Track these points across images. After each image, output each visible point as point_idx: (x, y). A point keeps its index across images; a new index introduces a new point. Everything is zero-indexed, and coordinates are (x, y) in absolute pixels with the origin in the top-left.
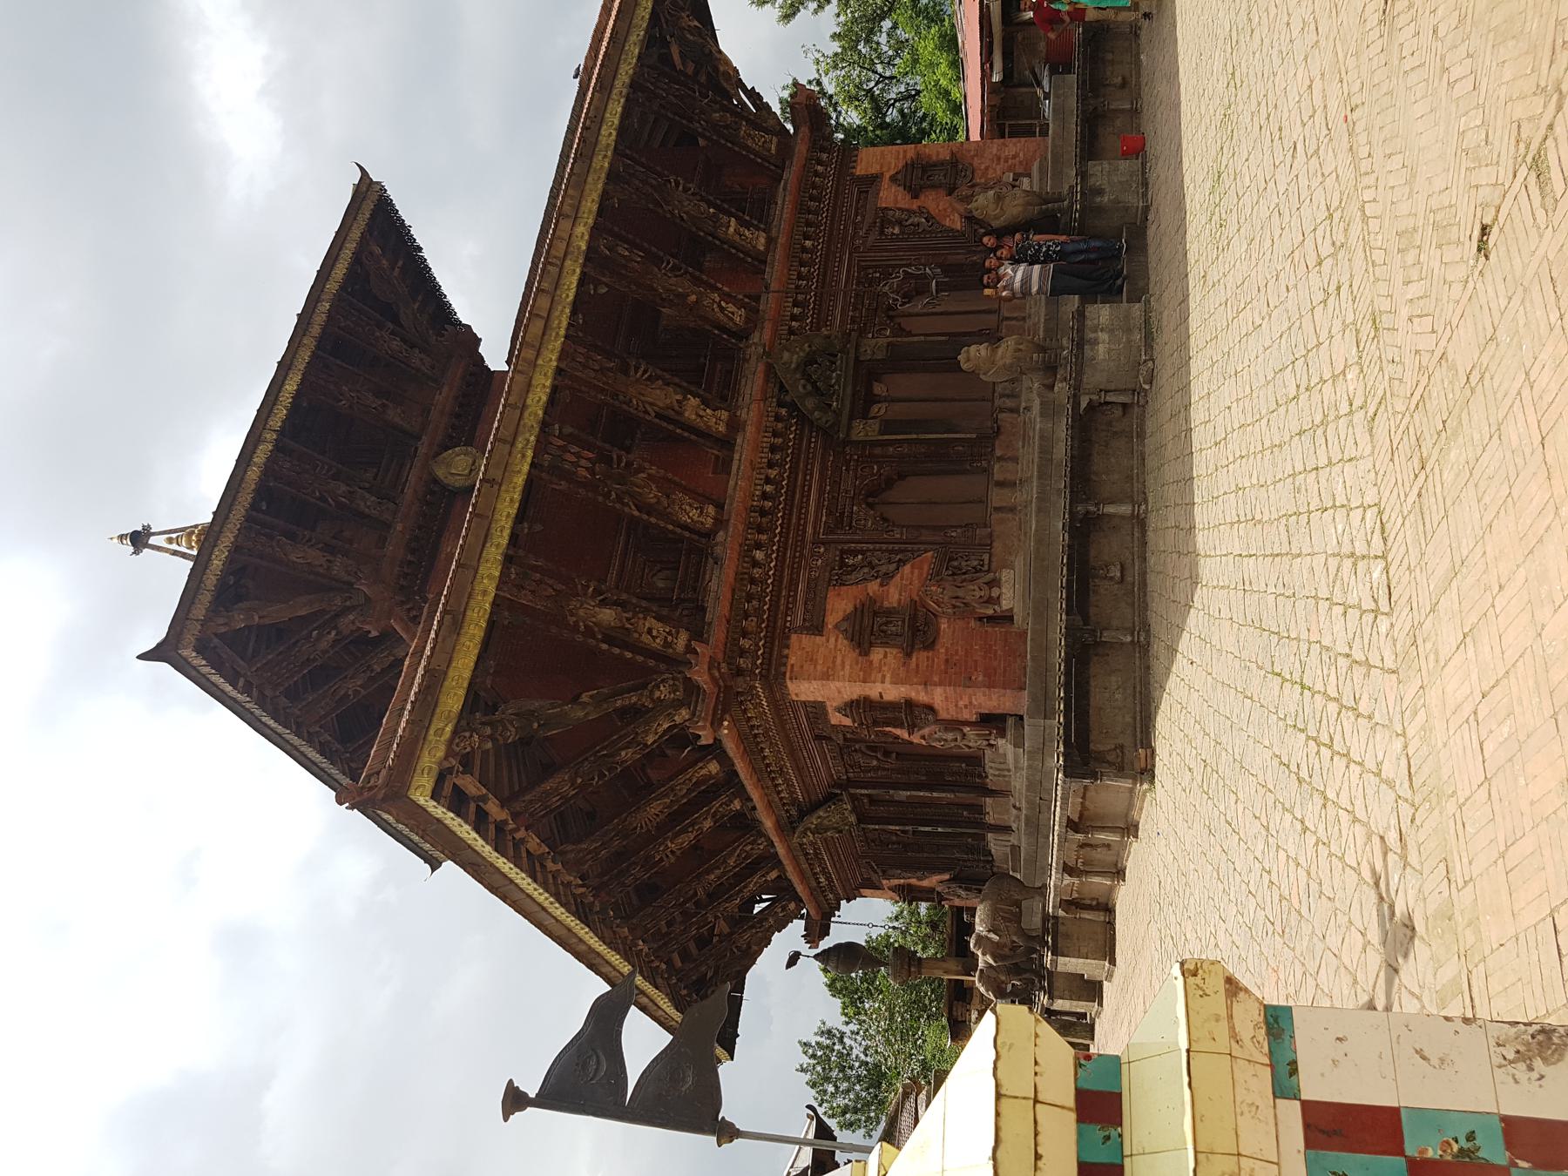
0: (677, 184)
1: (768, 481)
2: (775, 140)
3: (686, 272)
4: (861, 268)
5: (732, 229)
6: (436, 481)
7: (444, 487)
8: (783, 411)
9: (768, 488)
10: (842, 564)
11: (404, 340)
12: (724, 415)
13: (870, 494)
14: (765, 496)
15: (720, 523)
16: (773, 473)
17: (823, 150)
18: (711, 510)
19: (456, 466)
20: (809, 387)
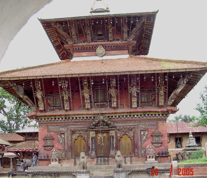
0: (138, 88)
1: (76, 118)
2: (163, 104)
3: (118, 94)
4: (134, 128)
5: (133, 100)
6: (97, 47)
7: (96, 49)
8: (92, 118)
9: (74, 118)
10: (62, 134)
11: (128, 31)
12: (89, 107)
13: (81, 136)
14: (73, 118)
15: (67, 111)
16: (78, 119)
17: (163, 115)
18: (68, 108)
19: (100, 50)
20: (97, 122)
